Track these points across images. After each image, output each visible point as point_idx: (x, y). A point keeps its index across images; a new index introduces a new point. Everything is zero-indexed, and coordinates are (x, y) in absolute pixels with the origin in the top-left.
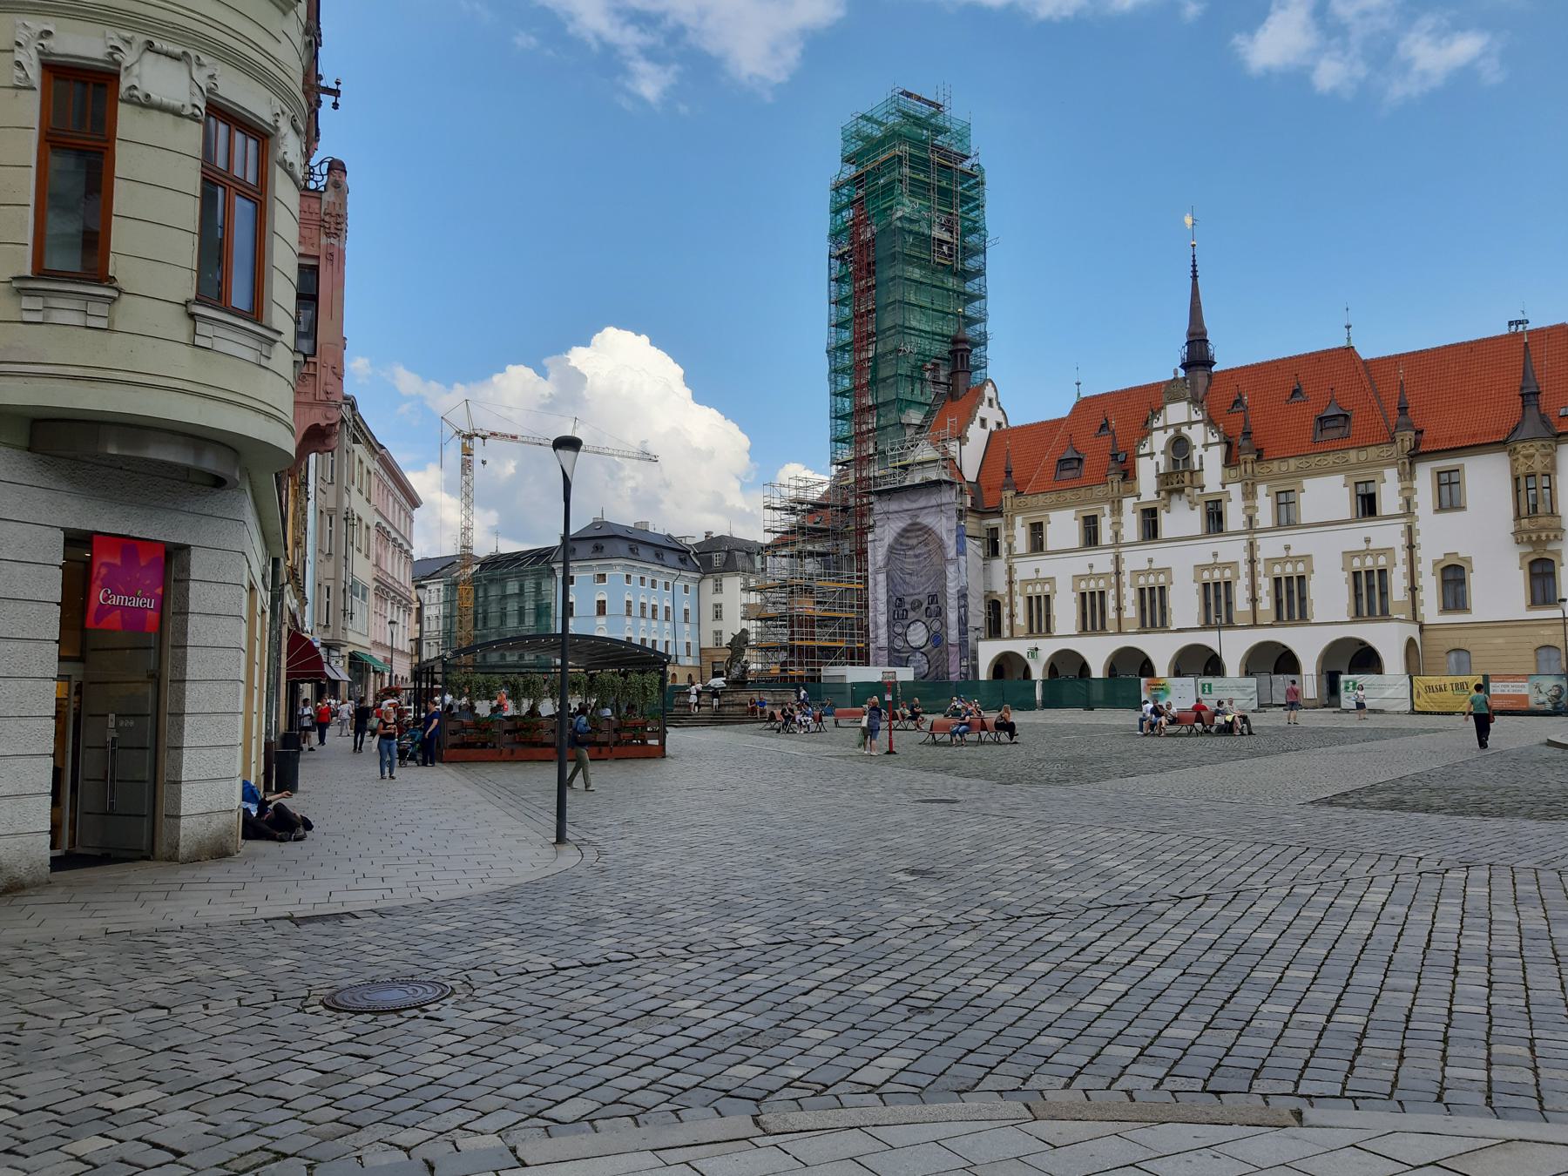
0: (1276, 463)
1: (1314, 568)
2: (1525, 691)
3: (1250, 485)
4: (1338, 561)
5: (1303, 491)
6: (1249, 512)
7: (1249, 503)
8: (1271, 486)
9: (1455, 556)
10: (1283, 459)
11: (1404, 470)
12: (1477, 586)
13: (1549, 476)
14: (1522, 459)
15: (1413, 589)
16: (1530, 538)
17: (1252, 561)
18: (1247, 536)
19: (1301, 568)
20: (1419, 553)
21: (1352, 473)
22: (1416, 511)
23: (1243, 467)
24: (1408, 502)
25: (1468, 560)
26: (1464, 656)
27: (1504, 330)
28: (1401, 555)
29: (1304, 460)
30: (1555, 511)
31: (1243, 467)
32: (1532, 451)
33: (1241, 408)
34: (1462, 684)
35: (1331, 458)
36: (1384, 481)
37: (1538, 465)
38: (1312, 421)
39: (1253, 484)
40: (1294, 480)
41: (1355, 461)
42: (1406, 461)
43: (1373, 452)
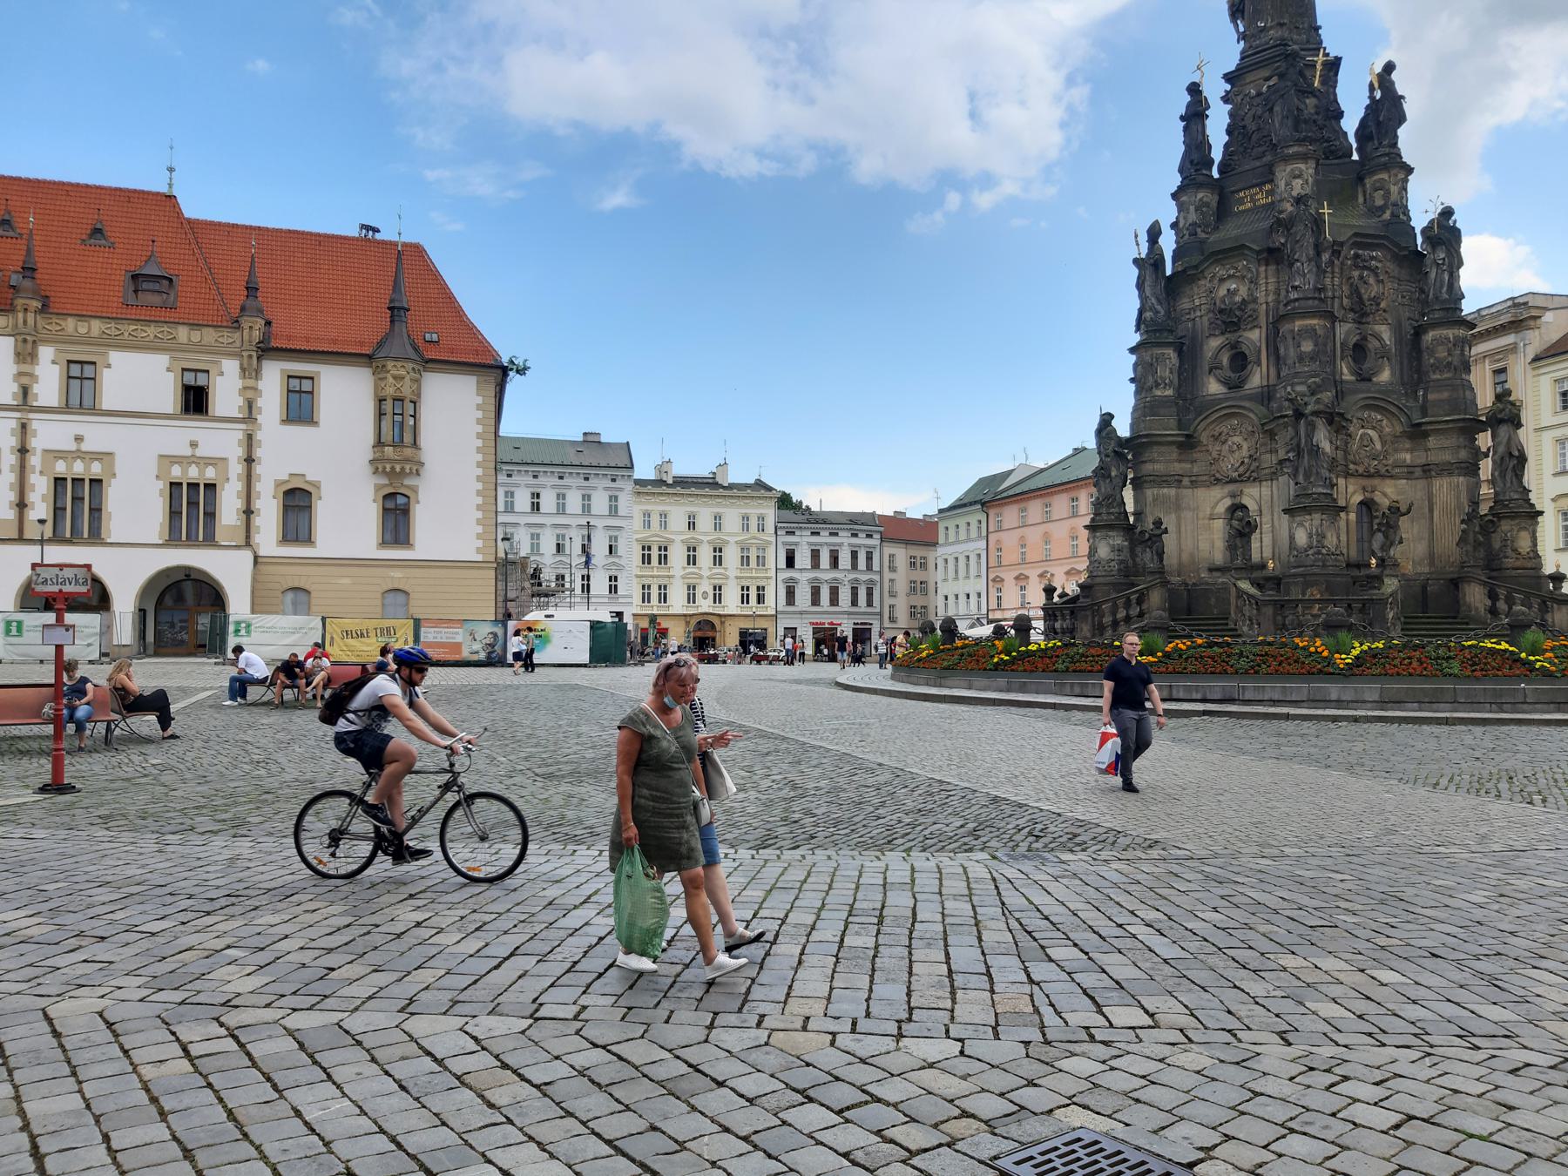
1: (117, 471)
2: (459, 639)
3: (29, 346)
6: (25, 380)
7: (25, 368)
11: (250, 364)
12: (324, 514)
13: (415, 403)
14: (391, 380)
15: (248, 512)
16: (393, 468)
17: (23, 451)
18: (17, 415)
19: (96, 469)
20: (258, 469)
21: (180, 355)
22: (259, 417)
23: (20, 315)
24: (250, 405)
25: (317, 485)
26: (302, 596)
27: (353, 232)
28: (236, 469)
29: (113, 325)
30: (418, 443)
31: (20, 315)
32: (402, 372)
33: (11, 234)
34: (388, 629)
35: (152, 331)
37: (407, 390)
38: (121, 278)
39: (34, 342)
40: (102, 349)
41: (185, 341)
42: (254, 354)
43: (209, 335)
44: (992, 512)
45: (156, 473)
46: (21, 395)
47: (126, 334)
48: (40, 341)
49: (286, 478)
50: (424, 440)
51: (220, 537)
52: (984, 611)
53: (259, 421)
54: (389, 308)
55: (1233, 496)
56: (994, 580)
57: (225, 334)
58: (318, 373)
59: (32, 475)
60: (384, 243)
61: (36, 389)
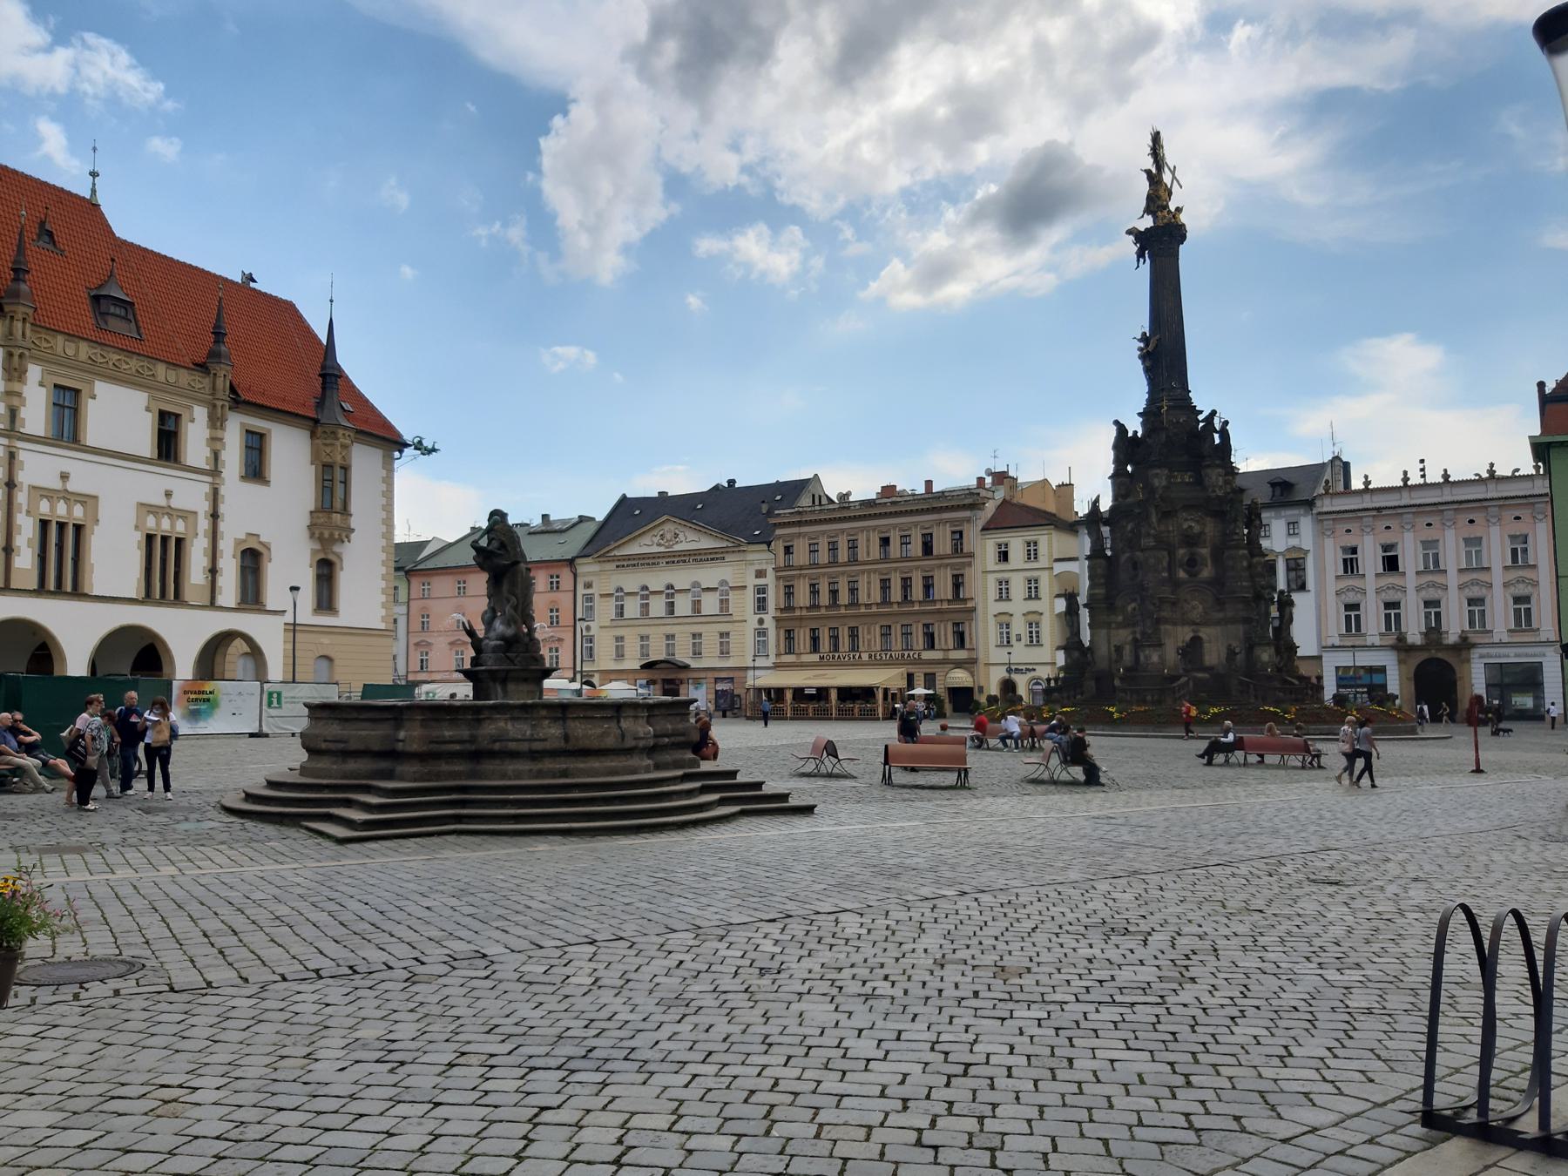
0: (60, 339)
1: (100, 517)
4: (131, 516)
5: (94, 397)
8: (50, 373)
9: (255, 538)
10: (71, 336)
15: (213, 571)
16: (331, 535)
19: (78, 512)
20: (222, 526)
24: (216, 456)
28: (204, 524)
29: (98, 351)
35: (134, 364)
36: (193, 421)
43: (184, 377)
44: (415, 582)
45: (134, 522)
46: (8, 419)
47: (111, 363)
48: (31, 357)
49: (243, 537)
50: (354, 507)
51: (189, 595)
52: (402, 671)
53: (223, 475)
54: (320, 375)
55: (1194, 631)
56: (417, 644)
57: (197, 378)
58: (269, 431)
59: (18, 515)
60: (260, 293)
61: (23, 413)
